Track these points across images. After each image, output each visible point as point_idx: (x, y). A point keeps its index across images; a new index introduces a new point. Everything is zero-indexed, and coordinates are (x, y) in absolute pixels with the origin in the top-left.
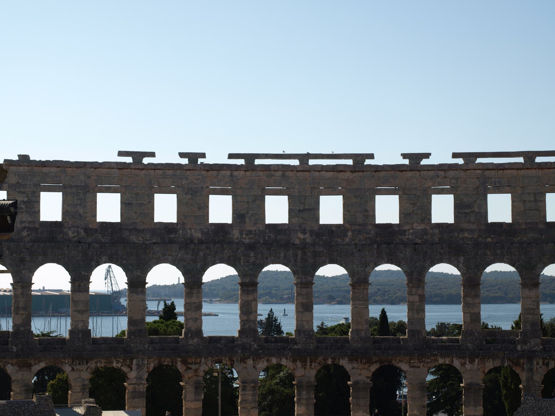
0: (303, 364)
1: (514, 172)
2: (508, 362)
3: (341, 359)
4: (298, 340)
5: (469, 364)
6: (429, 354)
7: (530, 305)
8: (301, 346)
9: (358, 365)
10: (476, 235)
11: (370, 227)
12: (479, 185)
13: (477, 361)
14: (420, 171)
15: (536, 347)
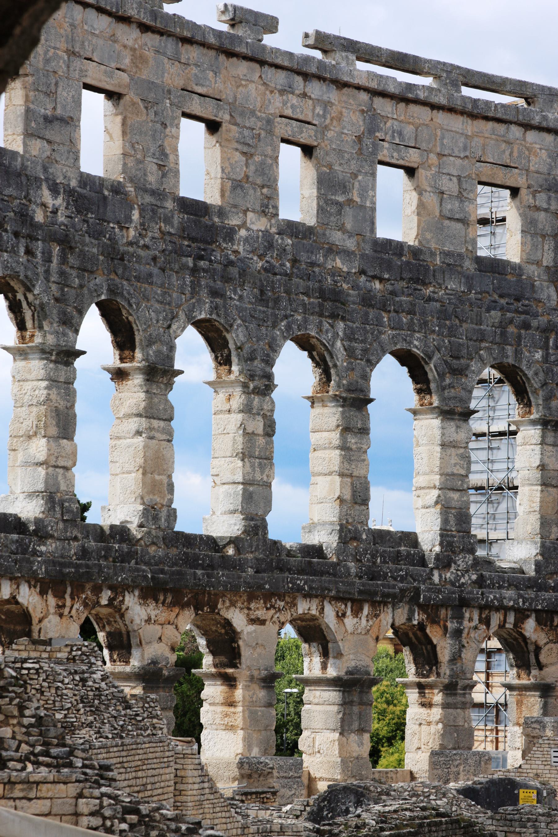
0: (60, 604)
1: (424, 113)
2: (419, 615)
3: (126, 593)
4: (50, 528)
5: (351, 617)
6: (290, 585)
7: (455, 465)
8: (54, 545)
9: (157, 612)
10: (355, 268)
11: (169, 205)
12: (363, 133)
13: (366, 610)
14: (262, 63)
15: (467, 577)
